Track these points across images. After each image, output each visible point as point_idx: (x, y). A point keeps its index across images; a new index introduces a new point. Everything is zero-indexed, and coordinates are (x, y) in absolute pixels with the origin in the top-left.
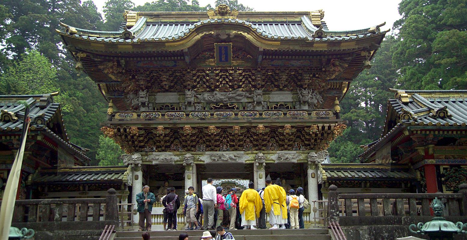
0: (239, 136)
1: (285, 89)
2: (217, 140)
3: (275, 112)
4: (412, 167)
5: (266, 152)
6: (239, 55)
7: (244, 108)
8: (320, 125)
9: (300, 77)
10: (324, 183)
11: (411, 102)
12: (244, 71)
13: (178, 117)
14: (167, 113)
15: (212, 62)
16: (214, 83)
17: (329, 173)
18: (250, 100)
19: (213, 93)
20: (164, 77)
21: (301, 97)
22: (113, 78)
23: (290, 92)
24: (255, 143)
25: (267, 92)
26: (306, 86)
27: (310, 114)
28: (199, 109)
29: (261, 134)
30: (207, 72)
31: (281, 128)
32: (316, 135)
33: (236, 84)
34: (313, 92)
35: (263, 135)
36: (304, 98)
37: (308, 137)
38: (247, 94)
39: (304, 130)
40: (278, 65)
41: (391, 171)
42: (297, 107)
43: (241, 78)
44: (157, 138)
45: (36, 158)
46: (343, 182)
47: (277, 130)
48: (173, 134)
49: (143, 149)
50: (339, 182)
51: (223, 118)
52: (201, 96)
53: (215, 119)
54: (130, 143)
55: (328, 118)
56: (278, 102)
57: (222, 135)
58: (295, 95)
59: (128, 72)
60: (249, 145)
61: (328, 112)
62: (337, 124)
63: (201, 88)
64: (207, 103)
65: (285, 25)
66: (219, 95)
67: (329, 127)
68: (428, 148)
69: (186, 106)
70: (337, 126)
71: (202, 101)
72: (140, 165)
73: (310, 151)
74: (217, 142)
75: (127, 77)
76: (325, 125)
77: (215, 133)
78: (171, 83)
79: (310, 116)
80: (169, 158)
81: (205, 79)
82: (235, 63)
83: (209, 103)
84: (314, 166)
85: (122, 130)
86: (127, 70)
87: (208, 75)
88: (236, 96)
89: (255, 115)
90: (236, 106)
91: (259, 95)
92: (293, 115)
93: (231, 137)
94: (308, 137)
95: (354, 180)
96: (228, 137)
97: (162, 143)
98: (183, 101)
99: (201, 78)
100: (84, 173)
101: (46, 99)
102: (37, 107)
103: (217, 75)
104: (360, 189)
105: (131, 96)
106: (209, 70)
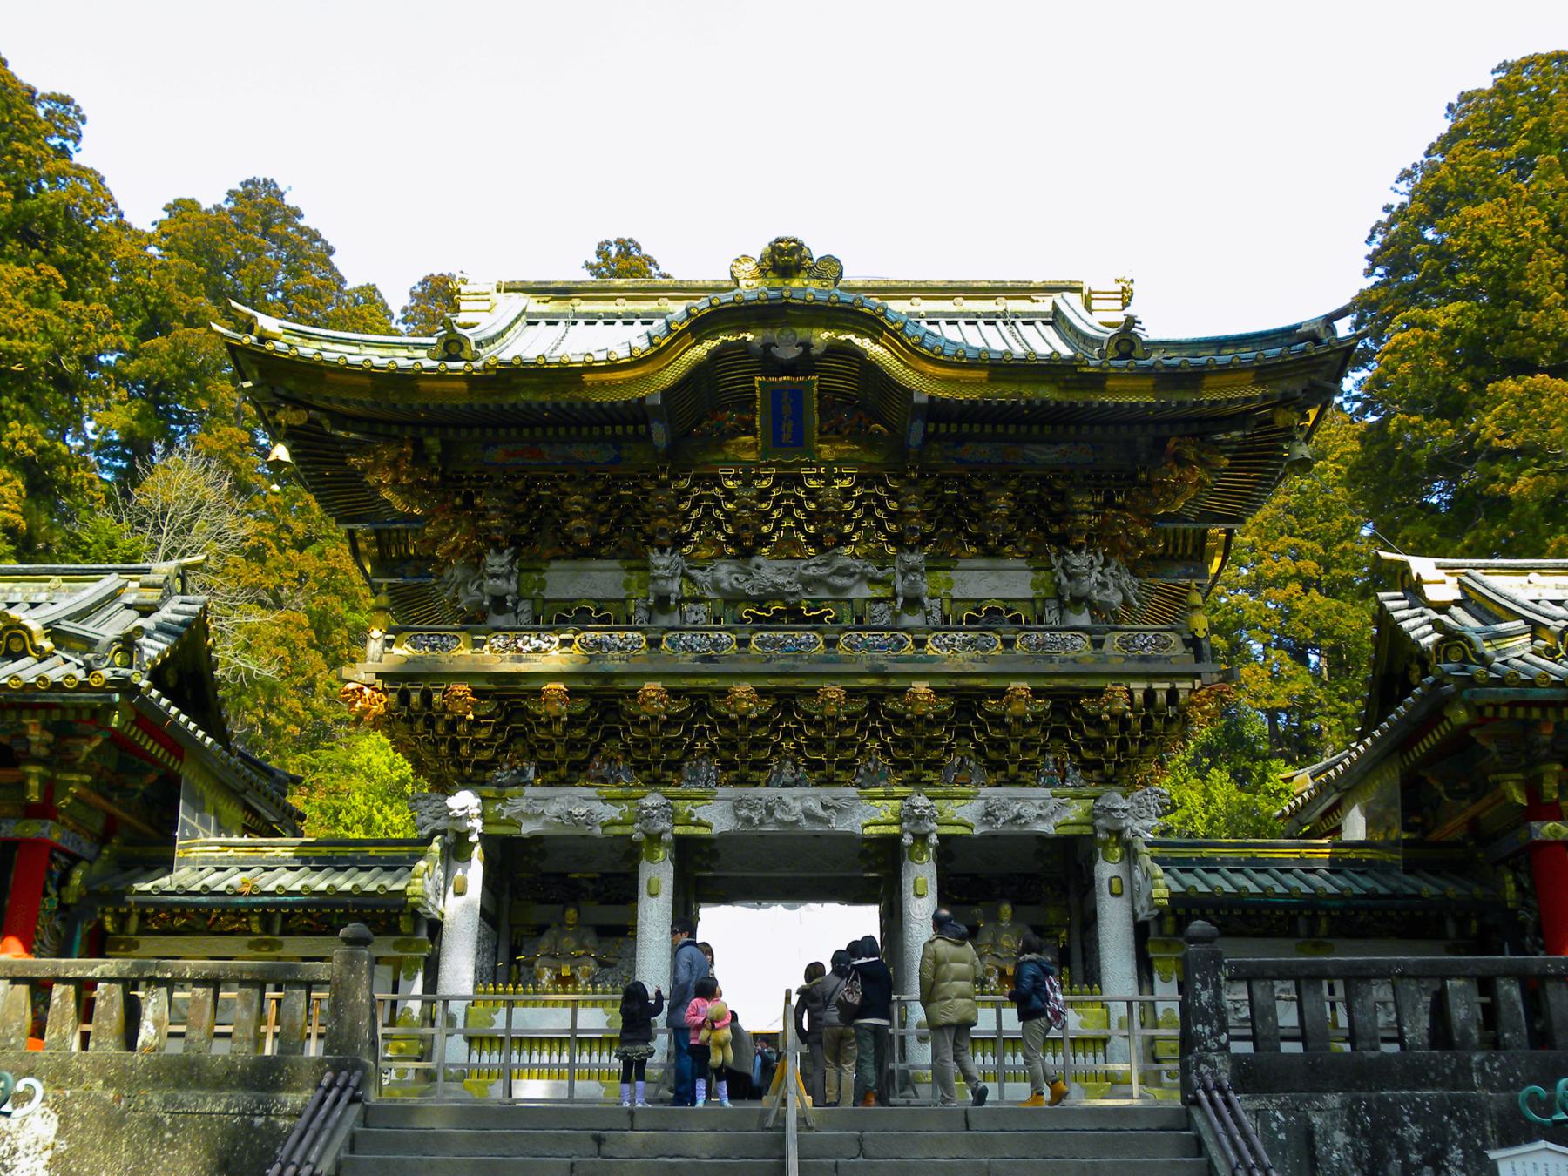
0: (841, 725)
1: (1008, 549)
2: (761, 744)
3: (971, 635)
4: (1480, 855)
5: (940, 791)
6: (841, 422)
7: (859, 620)
8: (1139, 687)
9: (1058, 505)
10: (1160, 918)
11: (1457, 603)
12: (861, 479)
13: (619, 649)
14: (582, 635)
15: (746, 449)
16: (754, 525)
17: (1177, 879)
18: (880, 592)
19: (748, 564)
20: (576, 501)
21: (1064, 580)
22: (399, 505)
23: (1023, 564)
24: (899, 754)
25: (940, 562)
26: (1082, 539)
27: (1097, 644)
28: (696, 622)
29: (920, 718)
30: (730, 483)
31: (992, 699)
32: (1124, 723)
33: (830, 530)
34: (1106, 564)
35: (929, 723)
36: (1073, 583)
37: (1092, 733)
38: (870, 569)
39: (1080, 706)
40: (982, 462)
41: (1406, 872)
42: (1052, 617)
43: (848, 506)
44: (542, 731)
45: (109, 800)
46: (1231, 912)
47: (980, 703)
48: (601, 717)
49: (488, 775)
50: (1217, 912)
51: (782, 657)
52: (705, 573)
53: (755, 658)
54: (443, 748)
55: (1167, 659)
56: (980, 600)
57: (779, 721)
58: (1043, 574)
59: (450, 482)
60: (876, 765)
61: (1165, 638)
62: (1198, 683)
63: (705, 545)
64: (727, 602)
65: (999, 323)
66: (770, 571)
67: (1172, 695)
68: (1539, 779)
69: (649, 609)
70: (1200, 689)
71: (709, 595)
72: (474, 838)
73: (1101, 788)
74: (760, 749)
75: (446, 500)
76: (1156, 686)
77: (754, 715)
78: (602, 523)
79: (1098, 650)
80: (580, 811)
81: (722, 510)
82: (827, 452)
83: (733, 599)
84: (1118, 851)
85: (415, 698)
86: (448, 473)
87: (730, 495)
88: (830, 575)
89: (901, 644)
90: (830, 614)
91: (913, 569)
92: (1038, 646)
93: (811, 732)
94: (1092, 733)
95: (1276, 906)
96: (799, 730)
97: (559, 750)
98: (642, 594)
99: (707, 506)
100: (270, 863)
101: (159, 579)
102: (128, 606)
103: (764, 495)
104: (1291, 942)
105: (456, 571)
106: (736, 477)
